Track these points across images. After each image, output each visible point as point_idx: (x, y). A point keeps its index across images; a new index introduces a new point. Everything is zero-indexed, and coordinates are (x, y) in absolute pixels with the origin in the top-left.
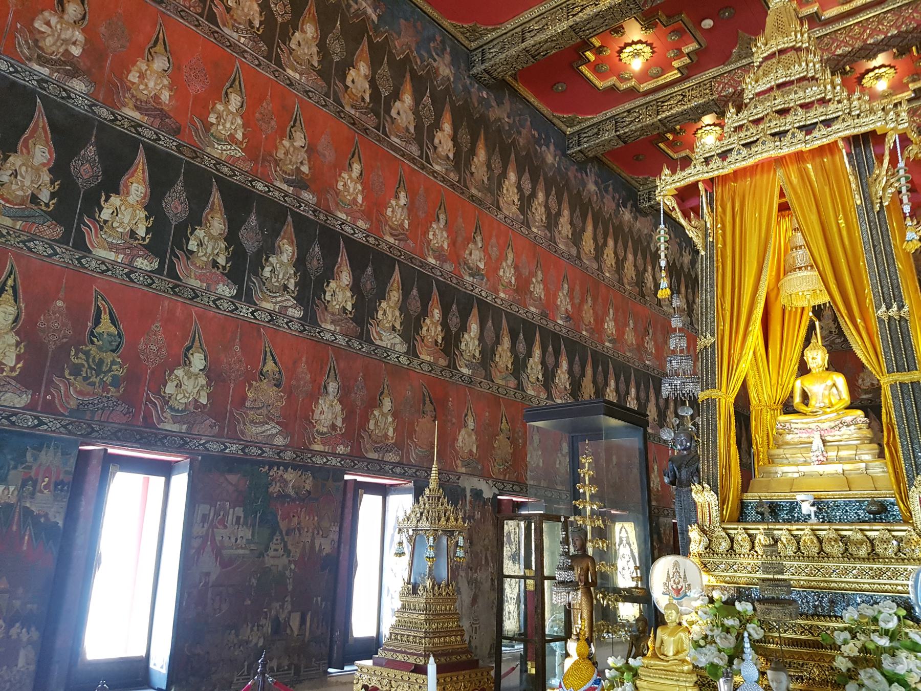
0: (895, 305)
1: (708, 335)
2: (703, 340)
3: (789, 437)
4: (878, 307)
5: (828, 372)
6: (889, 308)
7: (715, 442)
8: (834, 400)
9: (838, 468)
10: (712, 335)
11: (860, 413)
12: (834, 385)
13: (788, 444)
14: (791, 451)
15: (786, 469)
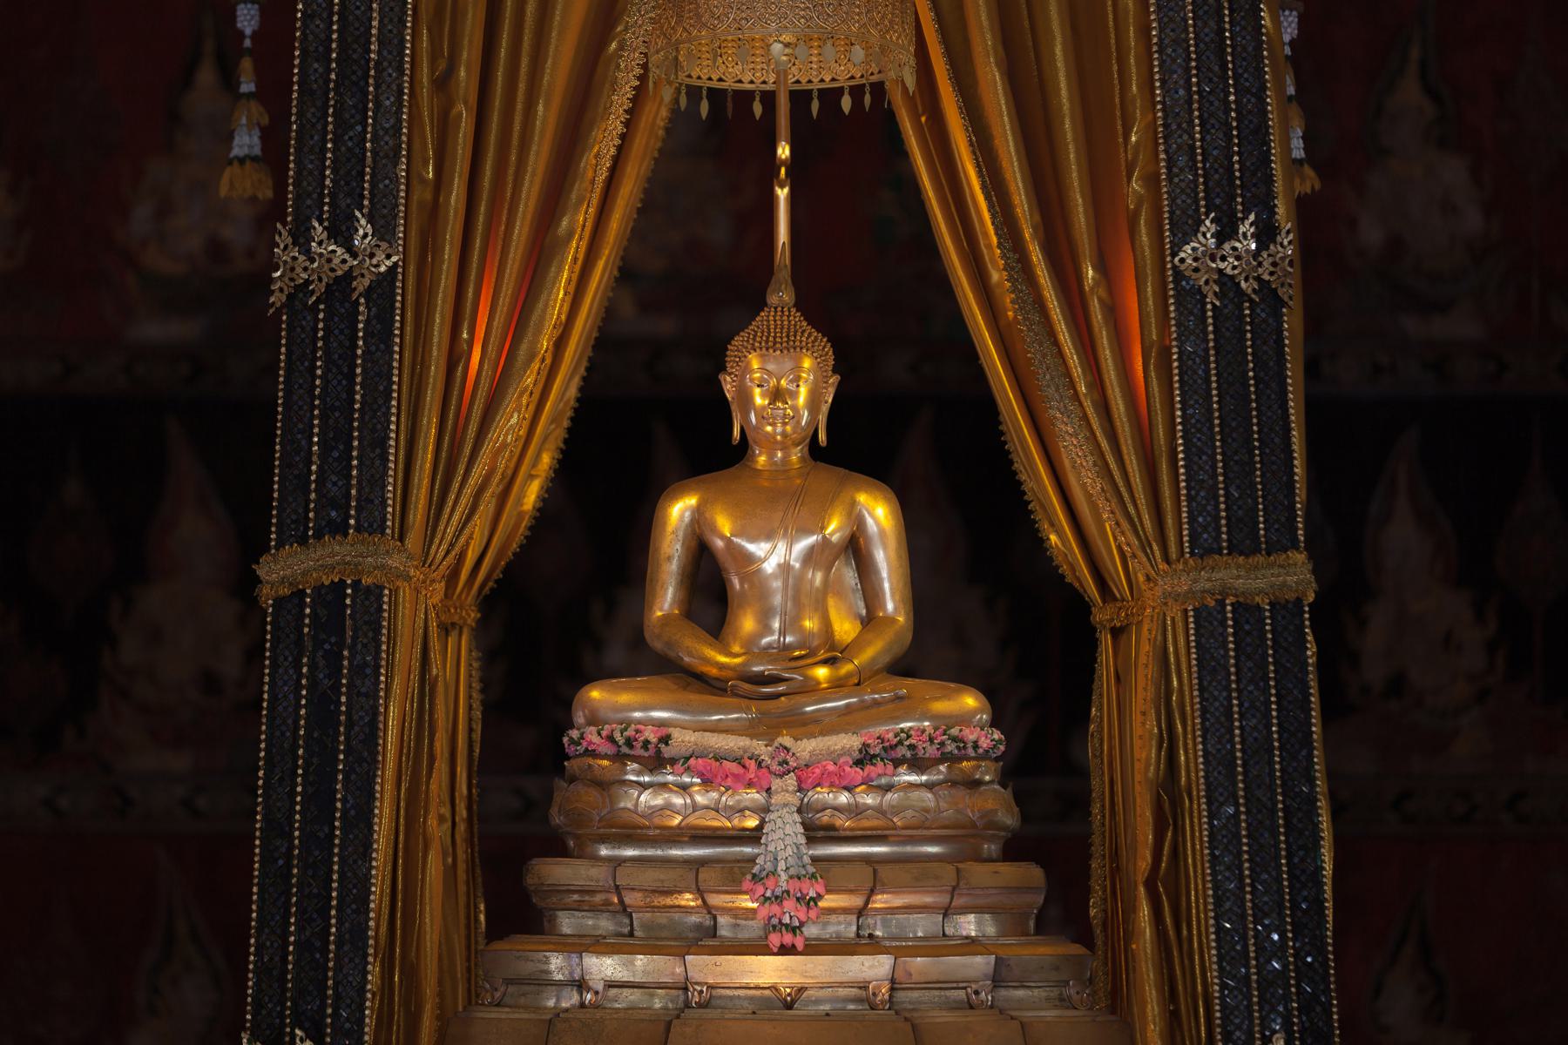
0: (1246, 228)
1: (364, 226)
2: (324, 246)
3: (645, 798)
4: (1186, 229)
5: (828, 475)
6: (1226, 233)
7: (361, 818)
8: (845, 628)
9: (874, 968)
10: (384, 231)
11: (970, 701)
12: (855, 547)
13: (631, 833)
14: (650, 877)
15: (604, 967)
